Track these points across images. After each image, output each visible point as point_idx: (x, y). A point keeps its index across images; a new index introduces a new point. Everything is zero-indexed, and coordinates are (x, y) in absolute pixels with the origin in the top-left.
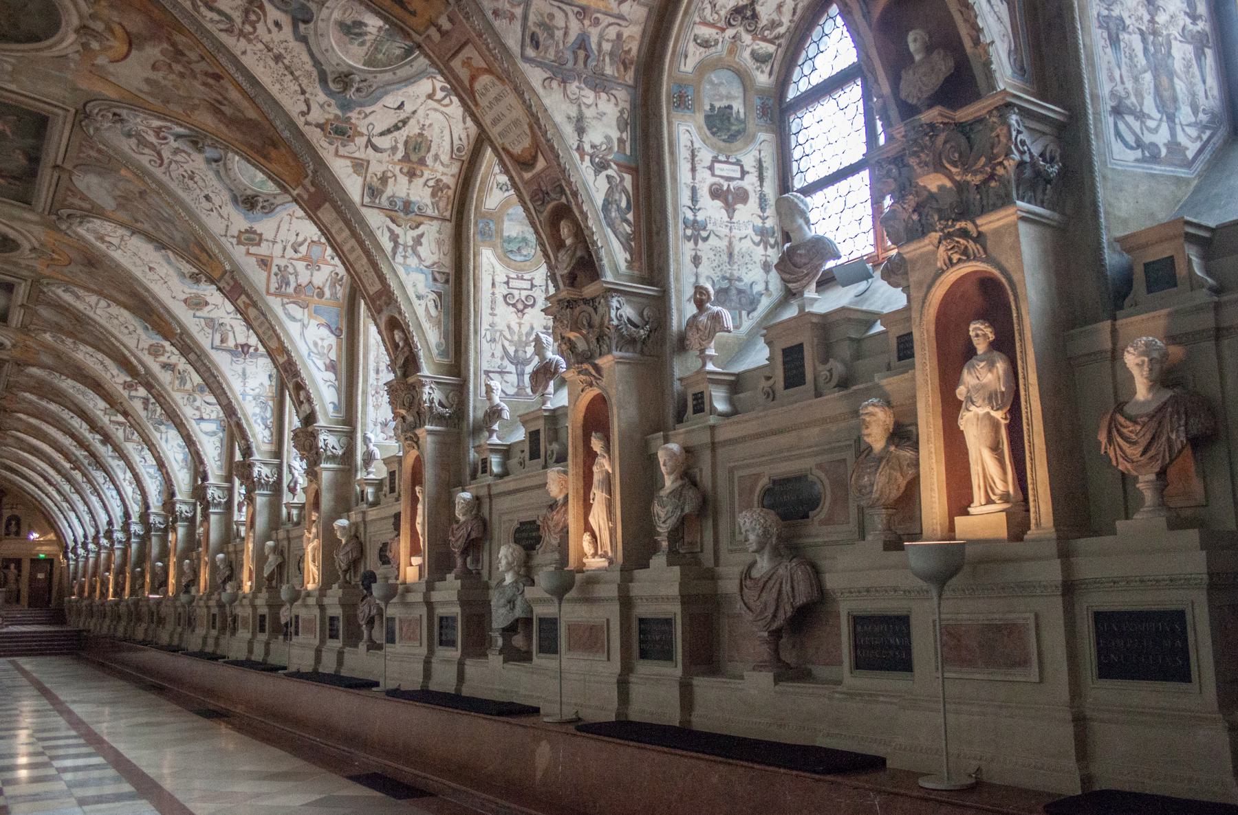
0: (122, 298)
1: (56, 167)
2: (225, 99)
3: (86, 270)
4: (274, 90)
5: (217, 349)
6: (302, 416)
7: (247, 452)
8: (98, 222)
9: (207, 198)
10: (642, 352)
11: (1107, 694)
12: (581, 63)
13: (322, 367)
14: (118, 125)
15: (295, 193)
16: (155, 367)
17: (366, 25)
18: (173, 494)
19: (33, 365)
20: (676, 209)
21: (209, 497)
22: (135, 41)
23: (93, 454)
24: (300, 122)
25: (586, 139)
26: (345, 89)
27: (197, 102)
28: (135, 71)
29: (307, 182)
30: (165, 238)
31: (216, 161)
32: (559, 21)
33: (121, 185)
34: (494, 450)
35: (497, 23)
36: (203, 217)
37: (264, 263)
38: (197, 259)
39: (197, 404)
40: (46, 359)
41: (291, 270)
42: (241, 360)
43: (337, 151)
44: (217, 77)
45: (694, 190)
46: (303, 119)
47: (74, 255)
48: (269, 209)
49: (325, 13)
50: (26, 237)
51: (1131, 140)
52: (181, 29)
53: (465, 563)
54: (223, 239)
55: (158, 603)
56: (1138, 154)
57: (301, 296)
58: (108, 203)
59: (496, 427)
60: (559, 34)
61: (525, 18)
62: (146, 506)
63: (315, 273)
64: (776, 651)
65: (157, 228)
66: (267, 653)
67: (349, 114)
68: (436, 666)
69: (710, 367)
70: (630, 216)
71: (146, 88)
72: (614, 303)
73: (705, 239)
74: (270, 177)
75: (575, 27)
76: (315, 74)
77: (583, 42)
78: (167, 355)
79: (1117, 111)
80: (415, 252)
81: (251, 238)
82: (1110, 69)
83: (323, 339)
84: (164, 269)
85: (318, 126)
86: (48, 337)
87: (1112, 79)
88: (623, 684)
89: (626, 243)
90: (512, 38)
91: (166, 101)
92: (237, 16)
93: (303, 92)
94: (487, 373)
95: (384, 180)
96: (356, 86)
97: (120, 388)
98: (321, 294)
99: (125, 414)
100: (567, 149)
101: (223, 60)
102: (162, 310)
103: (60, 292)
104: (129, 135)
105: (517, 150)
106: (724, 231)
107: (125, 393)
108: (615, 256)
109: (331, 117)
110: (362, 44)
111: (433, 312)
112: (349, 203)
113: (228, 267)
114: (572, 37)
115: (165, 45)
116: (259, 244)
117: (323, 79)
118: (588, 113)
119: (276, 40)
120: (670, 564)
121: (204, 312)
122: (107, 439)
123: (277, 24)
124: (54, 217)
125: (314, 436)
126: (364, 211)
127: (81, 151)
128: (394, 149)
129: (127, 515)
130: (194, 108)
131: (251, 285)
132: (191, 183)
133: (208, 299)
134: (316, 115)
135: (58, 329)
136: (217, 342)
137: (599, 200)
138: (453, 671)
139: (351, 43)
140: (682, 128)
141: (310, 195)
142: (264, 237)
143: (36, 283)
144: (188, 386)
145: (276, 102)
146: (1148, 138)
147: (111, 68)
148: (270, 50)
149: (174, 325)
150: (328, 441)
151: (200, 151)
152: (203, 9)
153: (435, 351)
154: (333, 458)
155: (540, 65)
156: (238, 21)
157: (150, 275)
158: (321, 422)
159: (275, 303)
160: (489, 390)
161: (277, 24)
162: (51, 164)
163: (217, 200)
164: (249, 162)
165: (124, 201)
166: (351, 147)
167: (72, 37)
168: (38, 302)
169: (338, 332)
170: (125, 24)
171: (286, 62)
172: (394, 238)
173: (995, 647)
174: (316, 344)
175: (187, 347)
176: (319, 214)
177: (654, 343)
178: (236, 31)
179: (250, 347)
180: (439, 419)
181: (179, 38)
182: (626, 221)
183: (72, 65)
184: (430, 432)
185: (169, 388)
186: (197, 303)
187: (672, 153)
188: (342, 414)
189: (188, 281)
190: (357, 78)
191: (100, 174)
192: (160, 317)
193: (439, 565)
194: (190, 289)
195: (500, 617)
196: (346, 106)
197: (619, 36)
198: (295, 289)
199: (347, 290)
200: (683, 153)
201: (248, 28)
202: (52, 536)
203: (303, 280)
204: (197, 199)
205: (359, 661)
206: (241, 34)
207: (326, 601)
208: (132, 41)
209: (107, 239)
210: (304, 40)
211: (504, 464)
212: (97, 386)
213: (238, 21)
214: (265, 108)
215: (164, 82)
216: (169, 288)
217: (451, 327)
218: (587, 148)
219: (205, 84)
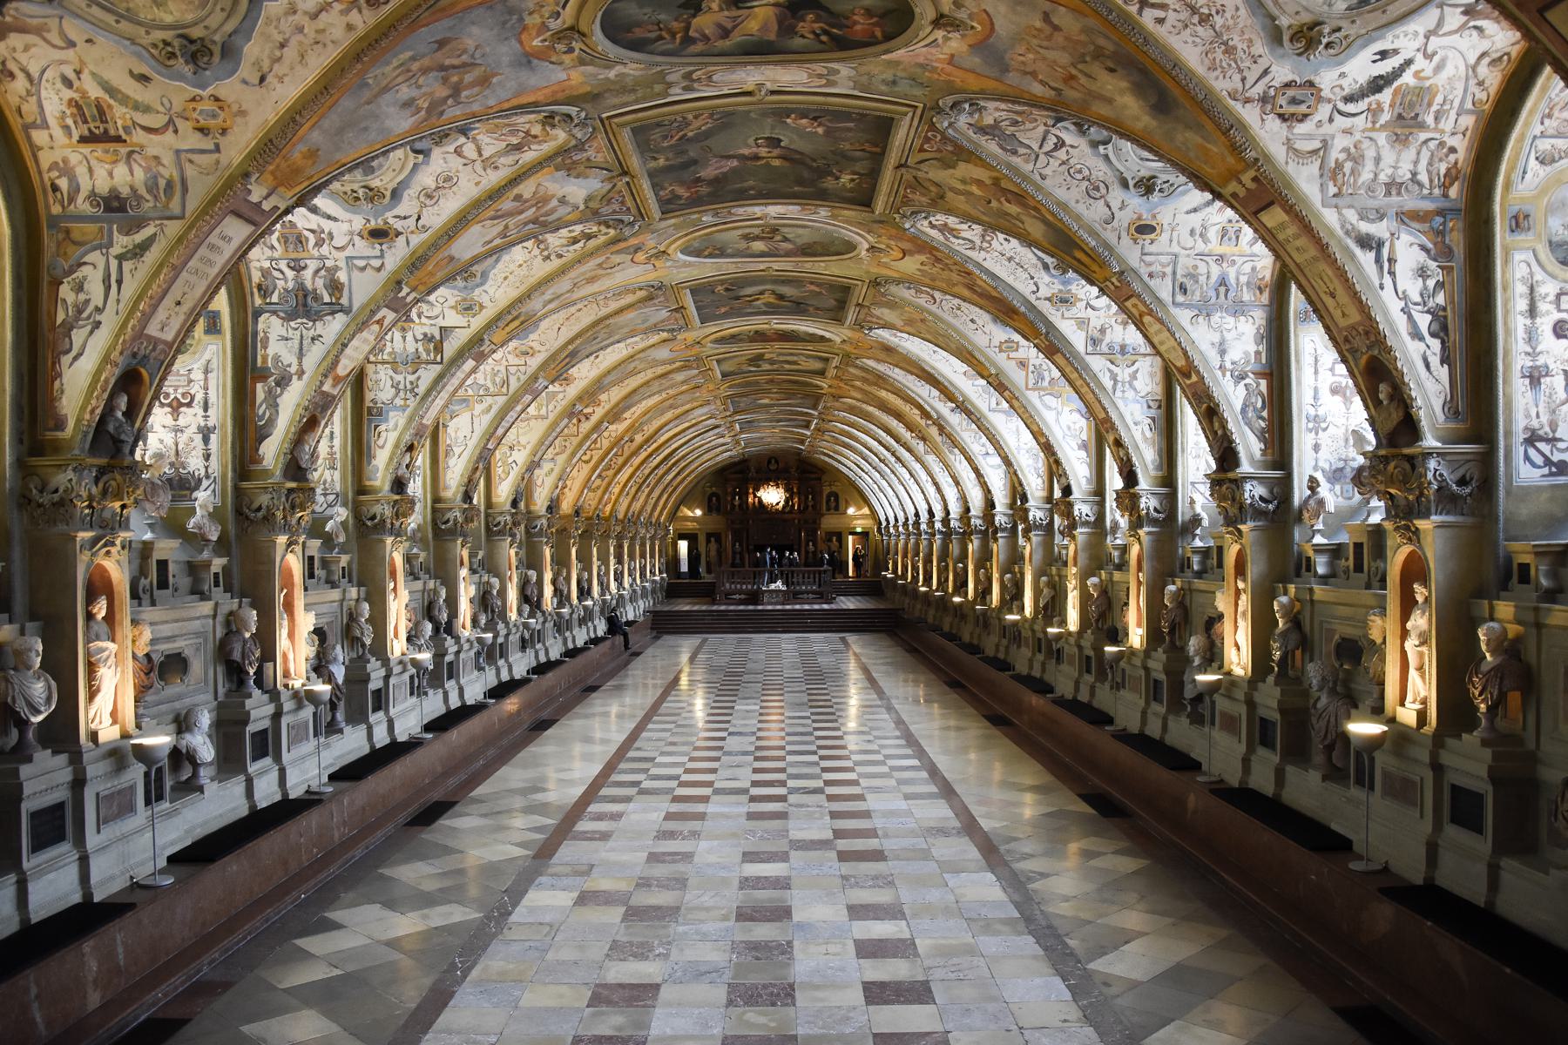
4: (1010, 280)
7: (1024, 498)
9: (972, 321)
10: (1273, 521)
11: (1452, 832)
12: (1222, 296)
18: (968, 510)
20: (1300, 410)
21: (997, 523)
23: (898, 459)
24: (1032, 298)
25: (1227, 358)
28: (911, 265)
32: (1202, 269)
34: (1196, 551)
35: (1152, 283)
36: (970, 334)
37: (1023, 364)
45: (1316, 389)
51: (1539, 460)
52: (937, 250)
53: (1172, 642)
55: (961, 604)
56: (1546, 471)
58: (899, 323)
59: (1198, 531)
60: (1202, 279)
61: (1174, 273)
62: (948, 513)
64: (1330, 759)
66: (1044, 670)
68: (1150, 716)
69: (1318, 539)
70: (1265, 414)
72: (1248, 487)
73: (1325, 430)
75: (1216, 271)
76: (1040, 265)
77: (1223, 282)
79: (1532, 439)
80: (1131, 385)
82: (1527, 410)
85: (1048, 299)
87: (1528, 416)
88: (1246, 762)
89: (1262, 438)
90: (1164, 290)
94: (1193, 484)
95: (1103, 331)
99: (924, 439)
100: (1211, 371)
105: (1179, 364)
106: (1344, 421)
107: (923, 422)
108: (1250, 447)
111: (1148, 434)
112: (1075, 354)
114: (1214, 278)
117: (1046, 267)
118: (1228, 336)
120: (1276, 684)
122: (909, 450)
125: (1070, 505)
126: (1089, 359)
128: (1109, 307)
129: (931, 513)
131: (1013, 384)
135: (865, 380)
136: (993, 405)
137: (1238, 406)
138: (1159, 723)
140: (1307, 339)
146: (1556, 457)
150: (1082, 509)
153: (1151, 467)
154: (1086, 524)
155: (1188, 306)
156: (978, 242)
158: (1077, 494)
159: (1033, 397)
160: (1192, 502)
162: (854, 301)
163: (980, 322)
166: (1074, 310)
167: (864, 253)
172: (1114, 378)
173: (1402, 790)
177: (1281, 514)
180: (1154, 522)
182: (1262, 418)
184: (1149, 533)
187: (1298, 361)
188: (1092, 487)
193: (1154, 636)
195: (1189, 693)
196: (1066, 283)
197: (1254, 269)
200: (1307, 360)
201: (985, 245)
202: (866, 511)
205: (1104, 699)
206: (981, 248)
207: (1083, 643)
211: (1203, 563)
212: (899, 416)
213: (978, 242)
217: (1164, 446)
218: (1228, 365)
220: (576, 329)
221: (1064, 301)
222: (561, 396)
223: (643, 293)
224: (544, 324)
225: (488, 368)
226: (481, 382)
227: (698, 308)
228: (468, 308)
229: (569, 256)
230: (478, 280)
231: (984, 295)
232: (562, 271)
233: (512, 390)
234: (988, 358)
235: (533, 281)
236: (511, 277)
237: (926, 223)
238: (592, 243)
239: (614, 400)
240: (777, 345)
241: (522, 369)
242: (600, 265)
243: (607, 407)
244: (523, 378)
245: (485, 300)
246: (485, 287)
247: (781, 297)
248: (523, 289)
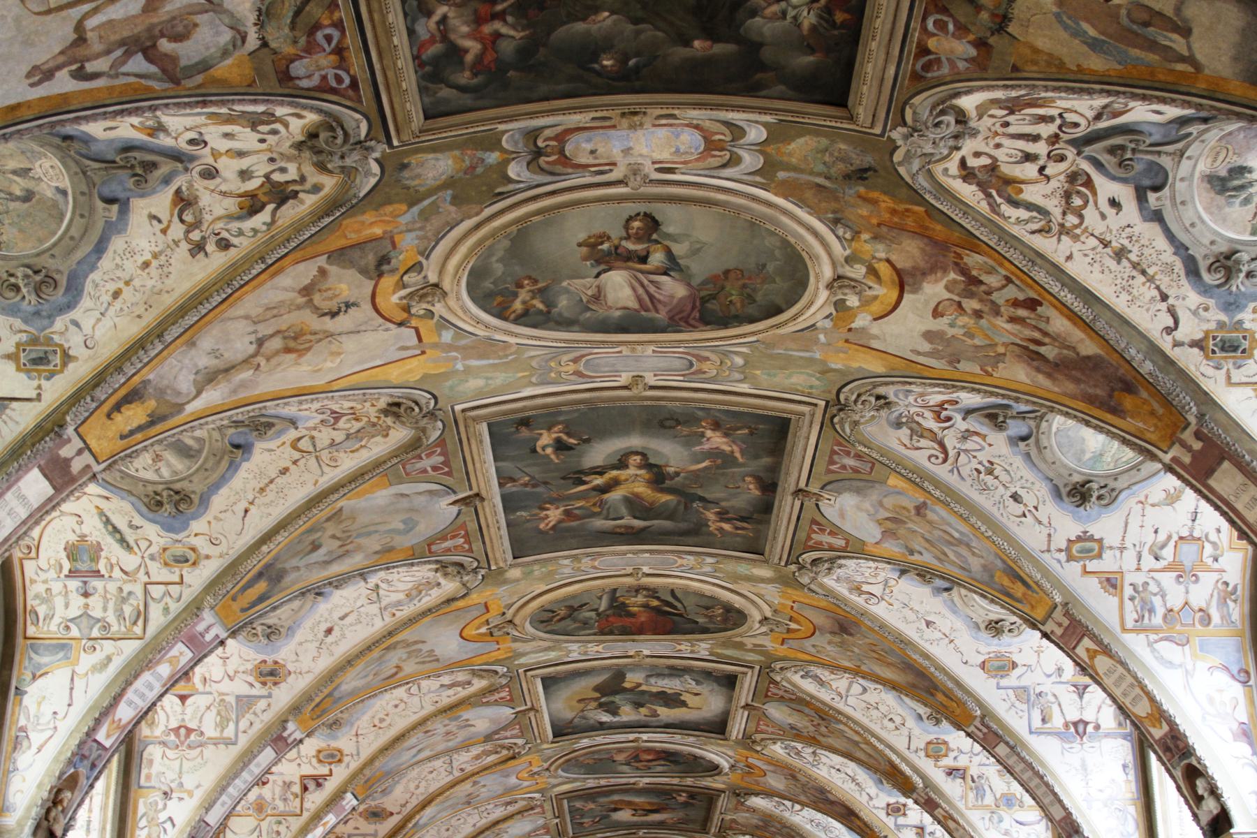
0: (888, 674)
1: (798, 492)
2: (1046, 334)
3: (837, 639)
4: (1120, 304)
5: (1038, 733)
6: (1205, 819)
8: (851, 563)
9: (1016, 497)
13: (1229, 736)
14: (884, 413)
15: (1167, 458)
16: (937, 775)
17: (1250, 171)
19: (757, 795)
22: (907, 279)
24: (1165, 344)
26: (1228, 279)
27: (1001, 350)
28: (908, 327)
29: (1187, 435)
30: (956, 572)
31: (1024, 439)
33: (889, 502)
37: (1112, 583)
38: (1009, 595)
39: (1006, 825)
40: (776, 782)
41: (1153, 588)
42: (1076, 746)
43: (1229, 377)
44: (1032, 304)
46: (1169, 339)
47: (819, 619)
48: (1109, 497)
49: (1186, 165)
50: (753, 602)
52: (973, 243)
54: (1046, 556)
57: (1175, 625)
63: (1192, 587)
65: (942, 557)
67: (1239, 317)
71: (926, 347)
74: (1125, 442)
76: (1179, 266)
78: (952, 755)
81: (1085, 548)
83: (1221, 691)
84: (948, 621)
85: (1198, 344)
86: (778, 749)
91: (954, 360)
92: (1054, 206)
93: (1164, 297)
96: (1245, 269)
97: (882, 814)
98: (1207, 620)
101: (1041, 276)
102: (950, 685)
103: (796, 678)
104: (898, 425)
107: (890, 821)
109: (1212, 326)
110: (1247, 201)
113: (1058, 599)
115: (952, 275)
116: (1099, 556)
117: (1192, 270)
119: (1114, 227)
121: (1012, 679)
123: (1114, 203)
124: (793, 567)
127: (832, 462)
130: (1000, 357)
132: (989, 479)
133: (1015, 658)
134: (1190, 329)
135: (797, 735)
136: (1037, 723)
139: (1230, 204)
141: (1196, 456)
142: (1106, 543)
143: (766, 671)
144: (989, 799)
145: (1127, 322)
147: (875, 329)
148: (1106, 244)
149: (971, 704)
151: (1000, 427)
152: (1006, 209)
156: (1056, 212)
157: (928, 633)
159: (1136, 645)
161: (1114, 203)
162: (792, 488)
164: (1088, 424)
165: (892, 525)
167: (824, 295)
168: (767, 697)
169: (1243, 677)
170: (893, 258)
171: (1133, 257)
174: (1211, 700)
175: (991, 736)
176: (1211, 482)
178: (1055, 228)
179: (1086, 723)
181: (973, 260)
183: (822, 337)
185: (961, 805)
186: (1000, 667)
189: (985, 635)
190: (1245, 257)
191: (858, 491)
192: (949, 695)
194: (989, 646)
196: (1231, 306)
198: (1165, 617)
199: (1247, 608)
201: (1072, 220)
203: (1175, 601)
204: (1001, 502)
206: (1064, 230)
208: (904, 282)
209: (865, 588)
210: (1157, 217)
213: (1056, 212)
214: (1111, 335)
215: (951, 332)
216: (956, 649)
219: (1012, 320)
220: (279, 511)
221: (1229, 347)
222: (262, 704)
223: (400, 434)
224: (219, 501)
225: (112, 587)
226: (97, 613)
227: (509, 503)
228: (39, 358)
229: (243, 245)
230: (59, 296)
231: (1067, 365)
232: (228, 287)
233: (152, 629)
234: (1046, 573)
235: (169, 301)
236: (127, 293)
237: (953, 166)
238: (291, 212)
239: (366, 754)
240: (649, 647)
241: (174, 590)
242: (307, 291)
243: (354, 765)
244: (175, 608)
245: (74, 342)
246: (76, 314)
247: (658, 477)
248: (150, 318)
